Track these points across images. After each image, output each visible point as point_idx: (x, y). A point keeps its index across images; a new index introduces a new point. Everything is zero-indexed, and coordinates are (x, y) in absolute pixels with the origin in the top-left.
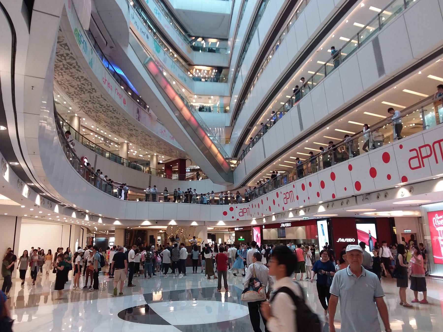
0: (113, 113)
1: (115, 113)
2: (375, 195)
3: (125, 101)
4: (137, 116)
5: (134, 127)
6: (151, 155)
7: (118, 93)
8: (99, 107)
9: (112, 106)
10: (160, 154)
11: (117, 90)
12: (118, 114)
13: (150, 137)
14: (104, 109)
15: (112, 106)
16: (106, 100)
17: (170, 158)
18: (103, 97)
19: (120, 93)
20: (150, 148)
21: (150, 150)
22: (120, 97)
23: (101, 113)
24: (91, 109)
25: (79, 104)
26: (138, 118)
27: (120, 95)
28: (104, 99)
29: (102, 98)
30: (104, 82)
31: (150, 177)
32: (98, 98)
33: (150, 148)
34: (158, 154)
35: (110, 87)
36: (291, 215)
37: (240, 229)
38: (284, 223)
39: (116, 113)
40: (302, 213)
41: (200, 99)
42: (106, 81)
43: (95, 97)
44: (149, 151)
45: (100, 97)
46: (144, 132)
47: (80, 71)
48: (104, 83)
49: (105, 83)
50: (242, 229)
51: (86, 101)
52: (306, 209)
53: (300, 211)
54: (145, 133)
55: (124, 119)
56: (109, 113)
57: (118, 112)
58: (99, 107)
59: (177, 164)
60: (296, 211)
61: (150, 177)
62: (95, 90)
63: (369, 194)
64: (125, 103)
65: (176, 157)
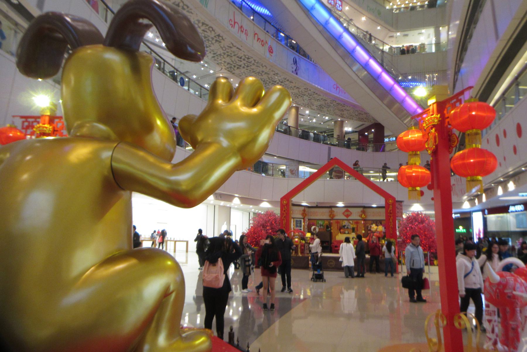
0: (257, 66)
1: (260, 66)
3: (272, 49)
4: (292, 68)
5: (292, 83)
6: (334, 120)
7: (258, 39)
8: (238, 60)
9: (252, 58)
11: (256, 36)
12: (265, 67)
14: (245, 62)
15: (252, 58)
16: (241, 50)
17: (361, 123)
18: (234, 45)
19: (262, 39)
22: (262, 44)
23: (245, 69)
24: (231, 65)
25: (215, 60)
26: (295, 70)
27: (262, 41)
28: (237, 48)
29: (235, 46)
30: (231, 24)
32: (231, 47)
34: (343, 119)
35: (244, 31)
38: (514, 205)
39: (260, 66)
42: (236, 24)
43: (227, 47)
45: (231, 46)
46: (308, 89)
47: (191, 13)
48: (232, 27)
49: (233, 26)
50: (459, 215)
51: (220, 55)
54: (310, 90)
55: (274, 73)
56: (253, 67)
57: (262, 64)
58: (238, 60)
59: (373, 130)
62: (221, 37)
64: (271, 51)
65: (368, 121)
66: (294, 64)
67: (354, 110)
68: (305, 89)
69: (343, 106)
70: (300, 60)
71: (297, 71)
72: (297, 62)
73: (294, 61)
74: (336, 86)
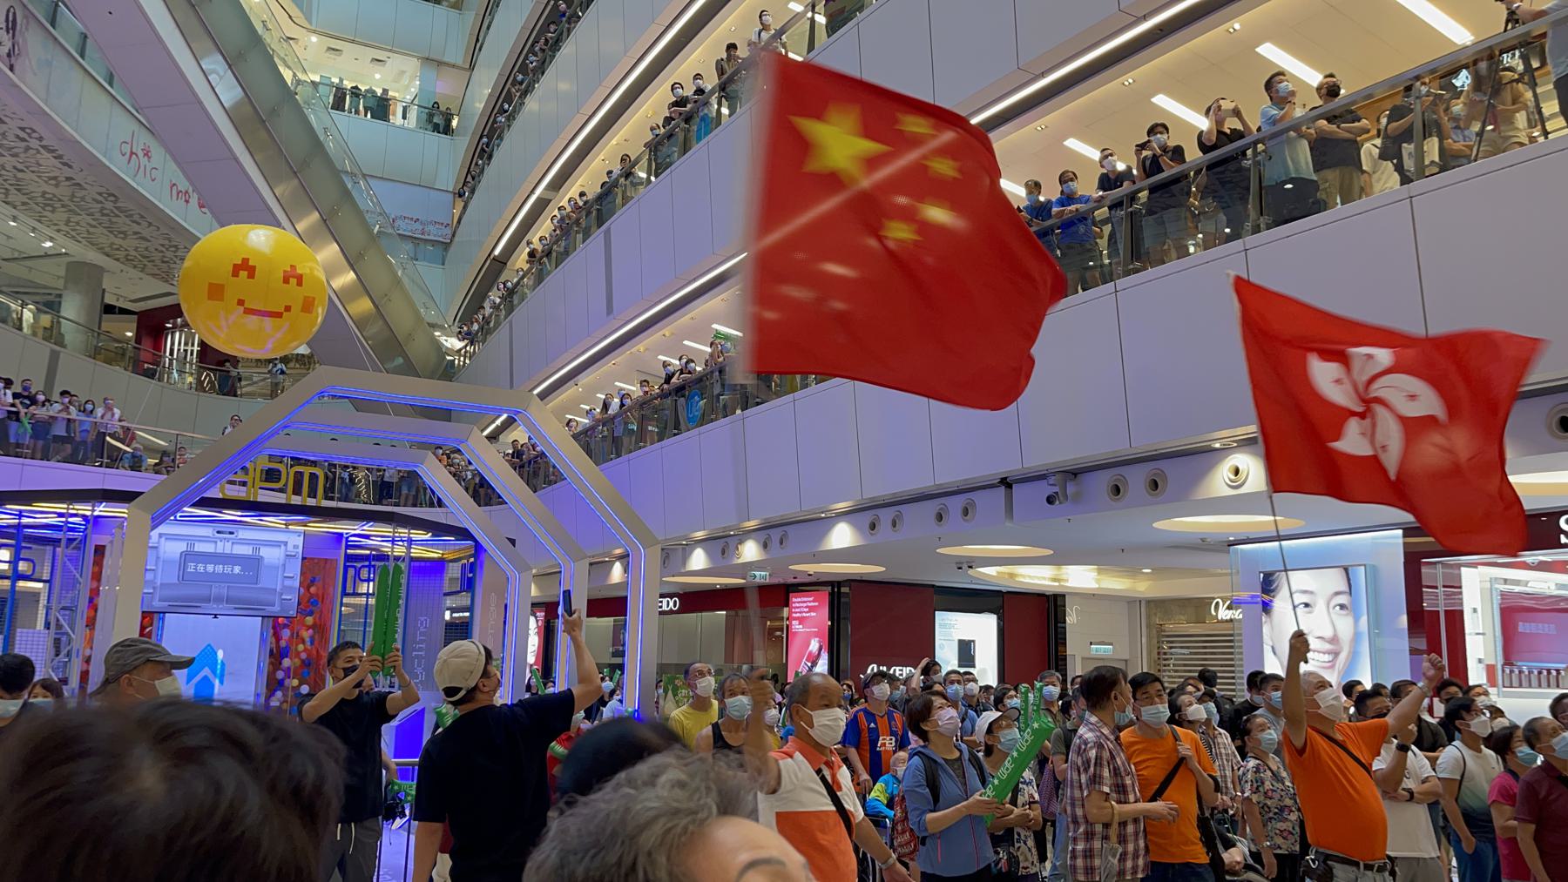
2: (1104, 479)
10: (117, 260)
13: (65, 164)
20: (67, 223)
21: (67, 234)
26: (9, 55)
31: (54, 357)
33: (67, 223)
36: (699, 559)
37: (455, 615)
40: (750, 551)
41: (331, 55)
44: (60, 238)
46: (34, 131)
52: (769, 532)
53: (741, 542)
54: (41, 139)
60: (722, 544)
61: (54, 357)
63: (1074, 474)
66: (8, 32)
67: (167, 242)
68: (23, 129)
69: (134, 222)
70: (28, 22)
71: (13, 59)
72: (18, 27)
73: (7, 20)
74: (127, 149)
